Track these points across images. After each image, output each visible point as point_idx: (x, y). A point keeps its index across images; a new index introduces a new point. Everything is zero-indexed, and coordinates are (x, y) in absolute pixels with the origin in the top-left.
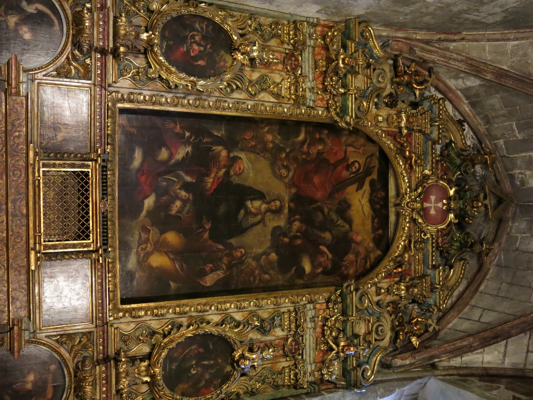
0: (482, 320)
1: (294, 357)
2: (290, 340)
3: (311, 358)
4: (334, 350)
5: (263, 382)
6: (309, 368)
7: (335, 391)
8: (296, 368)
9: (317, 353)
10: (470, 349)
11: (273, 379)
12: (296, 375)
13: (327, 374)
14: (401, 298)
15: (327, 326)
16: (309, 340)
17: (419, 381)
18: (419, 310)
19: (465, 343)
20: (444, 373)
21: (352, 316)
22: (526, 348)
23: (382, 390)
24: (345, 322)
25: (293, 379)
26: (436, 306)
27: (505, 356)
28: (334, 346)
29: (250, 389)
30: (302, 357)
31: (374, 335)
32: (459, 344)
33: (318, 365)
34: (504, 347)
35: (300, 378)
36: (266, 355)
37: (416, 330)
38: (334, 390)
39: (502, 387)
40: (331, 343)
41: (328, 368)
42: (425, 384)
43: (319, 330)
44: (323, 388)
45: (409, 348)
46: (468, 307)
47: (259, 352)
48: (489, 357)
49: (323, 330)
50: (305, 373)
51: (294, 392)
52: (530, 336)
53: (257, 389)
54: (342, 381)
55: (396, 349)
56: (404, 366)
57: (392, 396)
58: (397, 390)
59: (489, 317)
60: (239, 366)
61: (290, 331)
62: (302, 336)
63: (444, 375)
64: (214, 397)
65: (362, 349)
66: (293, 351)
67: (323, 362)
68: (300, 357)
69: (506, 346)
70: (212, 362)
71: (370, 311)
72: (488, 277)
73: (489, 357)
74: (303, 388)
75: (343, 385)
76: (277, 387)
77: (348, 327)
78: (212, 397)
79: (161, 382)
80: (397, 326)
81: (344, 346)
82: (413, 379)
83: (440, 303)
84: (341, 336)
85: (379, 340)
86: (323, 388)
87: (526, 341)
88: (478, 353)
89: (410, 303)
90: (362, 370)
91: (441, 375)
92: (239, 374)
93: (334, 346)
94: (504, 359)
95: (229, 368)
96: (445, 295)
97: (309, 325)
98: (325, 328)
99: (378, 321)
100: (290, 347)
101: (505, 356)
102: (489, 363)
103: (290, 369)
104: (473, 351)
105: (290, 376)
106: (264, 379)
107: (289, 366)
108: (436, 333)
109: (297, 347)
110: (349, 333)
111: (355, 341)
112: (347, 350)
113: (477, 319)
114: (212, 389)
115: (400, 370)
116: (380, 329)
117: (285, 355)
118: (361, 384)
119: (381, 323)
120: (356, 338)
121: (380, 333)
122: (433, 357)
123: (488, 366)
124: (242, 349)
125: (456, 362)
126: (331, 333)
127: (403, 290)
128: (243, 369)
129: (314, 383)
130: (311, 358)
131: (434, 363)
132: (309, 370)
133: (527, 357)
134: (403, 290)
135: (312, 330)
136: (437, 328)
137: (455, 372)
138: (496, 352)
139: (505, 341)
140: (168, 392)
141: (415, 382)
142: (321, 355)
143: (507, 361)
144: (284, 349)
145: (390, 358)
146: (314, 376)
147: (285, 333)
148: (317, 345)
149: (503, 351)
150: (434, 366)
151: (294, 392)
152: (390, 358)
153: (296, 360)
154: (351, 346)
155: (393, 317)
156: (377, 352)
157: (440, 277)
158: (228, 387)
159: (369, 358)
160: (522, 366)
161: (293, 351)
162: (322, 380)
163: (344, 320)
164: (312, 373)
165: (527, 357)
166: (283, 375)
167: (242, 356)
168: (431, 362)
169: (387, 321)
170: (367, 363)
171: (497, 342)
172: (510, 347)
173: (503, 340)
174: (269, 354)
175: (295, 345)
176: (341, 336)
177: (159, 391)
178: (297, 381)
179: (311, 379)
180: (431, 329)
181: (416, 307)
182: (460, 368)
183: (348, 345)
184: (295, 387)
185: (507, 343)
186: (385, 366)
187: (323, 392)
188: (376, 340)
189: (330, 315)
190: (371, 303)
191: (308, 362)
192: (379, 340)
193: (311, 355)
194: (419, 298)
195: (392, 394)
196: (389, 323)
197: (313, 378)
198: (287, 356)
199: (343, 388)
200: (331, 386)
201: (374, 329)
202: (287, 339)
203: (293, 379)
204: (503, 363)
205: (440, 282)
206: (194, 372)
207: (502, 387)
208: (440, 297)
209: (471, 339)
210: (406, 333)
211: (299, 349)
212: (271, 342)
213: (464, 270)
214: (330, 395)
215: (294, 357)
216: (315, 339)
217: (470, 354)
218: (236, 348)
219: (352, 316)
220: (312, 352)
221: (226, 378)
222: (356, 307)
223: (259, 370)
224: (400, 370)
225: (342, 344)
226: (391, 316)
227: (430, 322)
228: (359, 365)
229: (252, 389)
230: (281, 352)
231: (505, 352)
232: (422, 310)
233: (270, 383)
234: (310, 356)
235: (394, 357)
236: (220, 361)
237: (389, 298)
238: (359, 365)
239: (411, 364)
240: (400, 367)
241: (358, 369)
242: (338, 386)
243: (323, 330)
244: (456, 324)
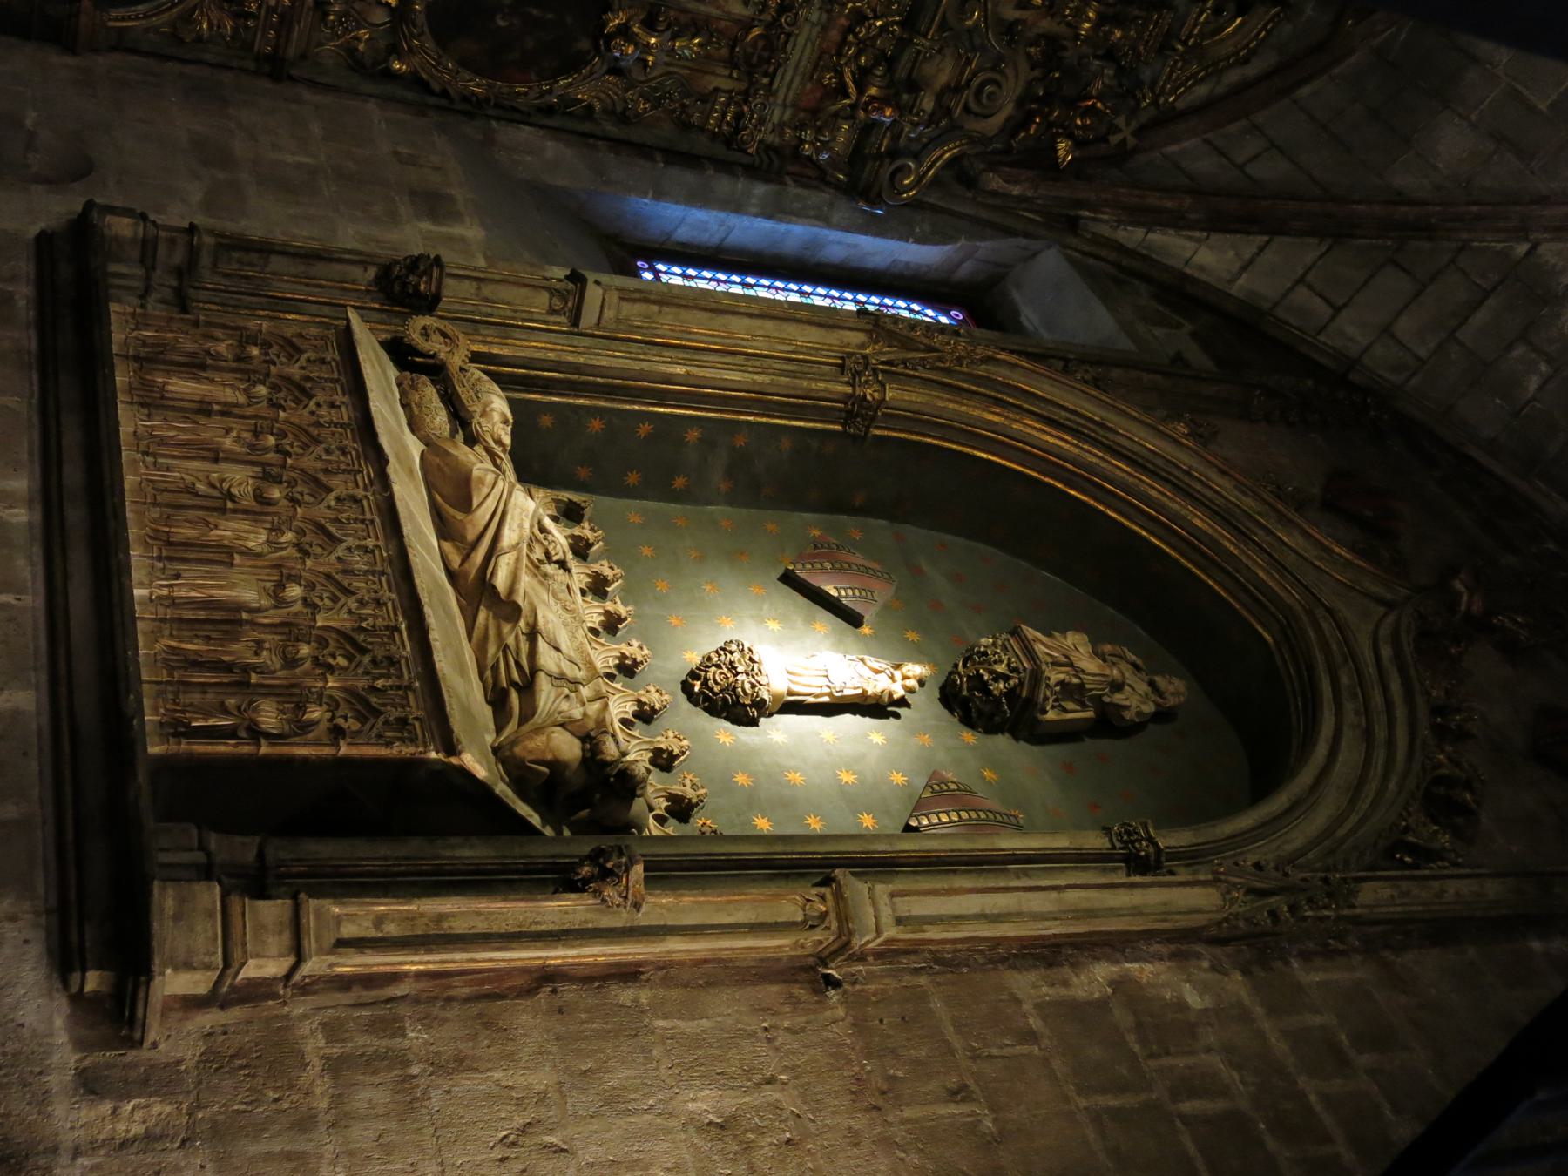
0: (1248, 170)
1: (750, 74)
2: (756, 32)
3: (791, 94)
4: (847, 96)
5: (656, 104)
6: (777, 113)
7: (816, 188)
8: (746, 101)
9: (809, 86)
10: (1177, 221)
11: (683, 106)
12: (739, 116)
13: (812, 143)
14: (1077, 36)
15: (856, 35)
16: (801, 49)
17: (1023, 241)
18: (1114, 83)
19: (1169, 204)
20: (1087, 248)
21: (925, 36)
22: (1300, 272)
23: (927, 227)
24: (902, 44)
25: (728, 124)
26: (1152, 89)
27: (1244, 268)
28: (852, 90)
29: (619, 108)
30: (771, 84)
31: (968, 95)
32: (1153, 200)
33: (802, 115)
34: (1255, 250)
35: (745, 128)
36: (682, 48)
37: (1078, 127)
38: (815, 183)
39: (1188, 327)
40: (848, 80)
41: (819, 131)
42: (1035, 254)
43: (834, 35)
44: (791, 168)
45: (1040, 161)
46: (1244, 122)
47: (668, 34)
48: (1208, 257)
49: (844, 42)
50: (761, 121)
51: (720, 151)
52: (1328, 250)
53: (638, 115)
54: (840, 171)
55: (1007, 151)
56: (1006, 196)
57: (947, 248)
58: (963, 241)
59: (1272, 170)
60: (608, 49)
61: (761, 12)
62: (789, 35)
63: (1084, 253)
64: (532, 95)
65: (912, 123)
66: (755, 60)
67: (815, 112)
68: (765, 81)
69: (1261, 249)
70: (549, 16)
71: (977, 41)
72: (1336, 71)
73: (1208, 257)
74: (745, 151)
75: (838, 180)
76: (685, 126)
77: (905, 57)
78: (526, 94)
79: (421, 19)
80: (1038, 100)
81: (873, 98)
82: (1009, 232)
83: (1164, 86)
84: (879, 71)
85: (976, 115)
86: (791, 168)
87: (1310, 257)
88: (1190, 238)
89: (1096, 57)
90: (894, 166)
91: (1076, 250)
92: (605, 68)
93: (852, 90)
94: (1239, 275)
95: (584, 44)
96: (1188, 73)
97: (815, 16)
98: (851, 38)
99: (993, 69)
100: (750, 50)
101: (1244, 268)
102: (1201, 268)
103: (730, 99)
104: (1182, 228)
105: (724, 115)
106: (661, 98)
107: (730, 92)
108: (1122, 155)
109: (766, 54)
110: (901, 73)
111: (905, 97)
112: (875, 109)
113: (1239, 160)
114: (533, 76)
115: (990, 201)
116: (988, 88)
117: (731, 63)
118: (879, 195)
119: (997, 77)
120: (909, 92)
121: (984, 101)
122: (1081, 204)
123: (1196, 274)
124: (632, 12)
125: (1132, 236)
126: (857, 56)
127: (1088, 20)
128: (617, 59)
129: (776, 150)
130: (791, 94)
131: (1079, 218)
132: (776, 118)
133: (1292, 289)
134: (1088, 20)
135: (818, 28)
136: (1131, 141)
137: (1112, 256)
138: (1231, 253)
139: (1266, 238)
140: (430, 45)
141: (1012, 241)
142: (818, 95)
143: (1241, 282)
144: (733, 48)
145: (982, 166)
146: (782, 134)
147: (748, 12)
148: (815, 68)
149: (1247, 256)
150: (1073, 225)
151: (720, 151)
152: (982, 166)
153: (751, 84)
154: (889, 105)
155: (1037, 73)
156: (951, 141)
157: (1195, 26)
158: (571, 84)
159: (925, 146)
160: (1266, 305)
161: (755, 60)
162: (796, 154)
163: (901, 39)
164: (779, 128)
165: (1292, 289)
166: (708, 106)
167: (624, 31)
168: (1072, 213)
169: (1017, 77)
170: (916, 157)
171: (1249, 233)
172: (1268, 256)
173: (1262, 233)
174: (688, 47)
175: (764, 49)
176: (879, 71)
177: (413, 36)
178: (737, 131)
179: (770, 138)
180: (1115, 139)
181: (1109, 72)
182: (1132, 253)
183: (883, 101)
184: (729, 142)
185: (1268, 242)
186: (960, 174)
187: (788, 179)
188: (967, 109)
189: (874, 11)
190: (986, 22)
191: (780, 101)
192: (976, 115)
193: (794, 86)
194: (1126, 55)
195: (945, 243)
196: (1021, 83)
197: (777, 140)
198: (736, 67)
199: (837, 186)
200: (812, 173)
201: (976, 82)
202: (747, 26)
203: (728, 124)
204: (1232, 282)
205: (1189, 37)
206: (501, 23)
207: (1188, 327)
208: (1171, 72)
209: (1188, 202)
210: (1050, 125)
211: (768, 62)
212: (708, 19)
213: (1269, 33)
214: (799, 191)
215: (750, 74)
216: (815, 55)
217: (1172, 232)
218: (616, 7)
219: (925, 36)
220: (797, 80)
221: (572, 64)
222: (944, 18)
223: (655, 73)
224: (990, 201)
225: (873, 91)
226: (1032, 69)
227: (1120, 121)
228: (893, 154)
229: (626, 109)
230: (724, 52)
231: (1251, 261)
232: (1121, 85)
233: (674, 111)
234: (789, 88)
235: (993, 167)
236: (569, 20)
237: (1046, 25)
238: (893, 154)
239: (1021, 199)
240: (994, 194)
241: (887, 161)
242: (828, 178)
243: (844, 42)
244: (1191, 153)
